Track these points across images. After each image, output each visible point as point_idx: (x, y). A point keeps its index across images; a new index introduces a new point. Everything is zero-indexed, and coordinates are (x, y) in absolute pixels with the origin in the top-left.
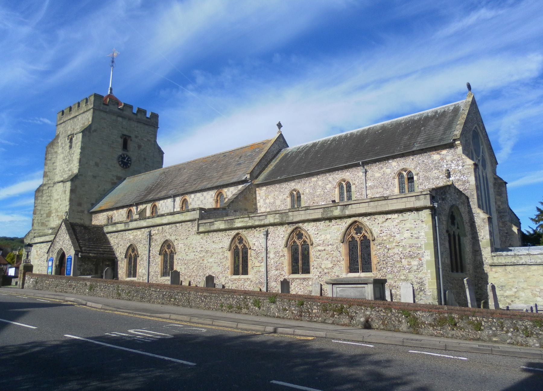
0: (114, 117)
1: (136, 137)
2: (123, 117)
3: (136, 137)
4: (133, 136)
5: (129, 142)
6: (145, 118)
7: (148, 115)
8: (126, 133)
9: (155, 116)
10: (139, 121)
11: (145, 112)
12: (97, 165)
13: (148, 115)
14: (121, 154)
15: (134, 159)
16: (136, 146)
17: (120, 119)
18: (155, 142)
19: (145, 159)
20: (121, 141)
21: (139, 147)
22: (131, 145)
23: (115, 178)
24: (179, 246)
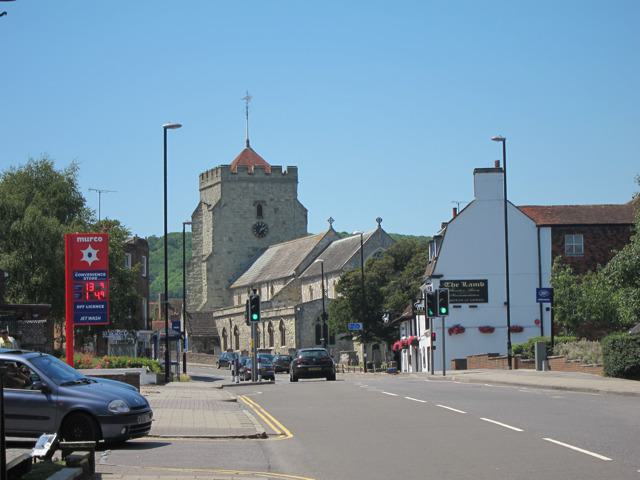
0: (244, 184)
1: (272, 200)
2: (255, 181)
3: (272, 200)
4: (267, 200)
5: (264, 207)
6: (280, 176)
7: (284, 169)
8: (259, 198)
9: (293, 170)
10: (273, 181)
11: (280, 168)
12: (230, 240)
13: (284, 169)
14: (254, 223)
15: (270, 225)
16: (273, 210)
17: (251, 185)
18: (296, 199)
19: (284, 223)
20: (254, 209)
21: (276, 210)
22: (266, 211)
23: (250, 250)
24: (240, 329)
